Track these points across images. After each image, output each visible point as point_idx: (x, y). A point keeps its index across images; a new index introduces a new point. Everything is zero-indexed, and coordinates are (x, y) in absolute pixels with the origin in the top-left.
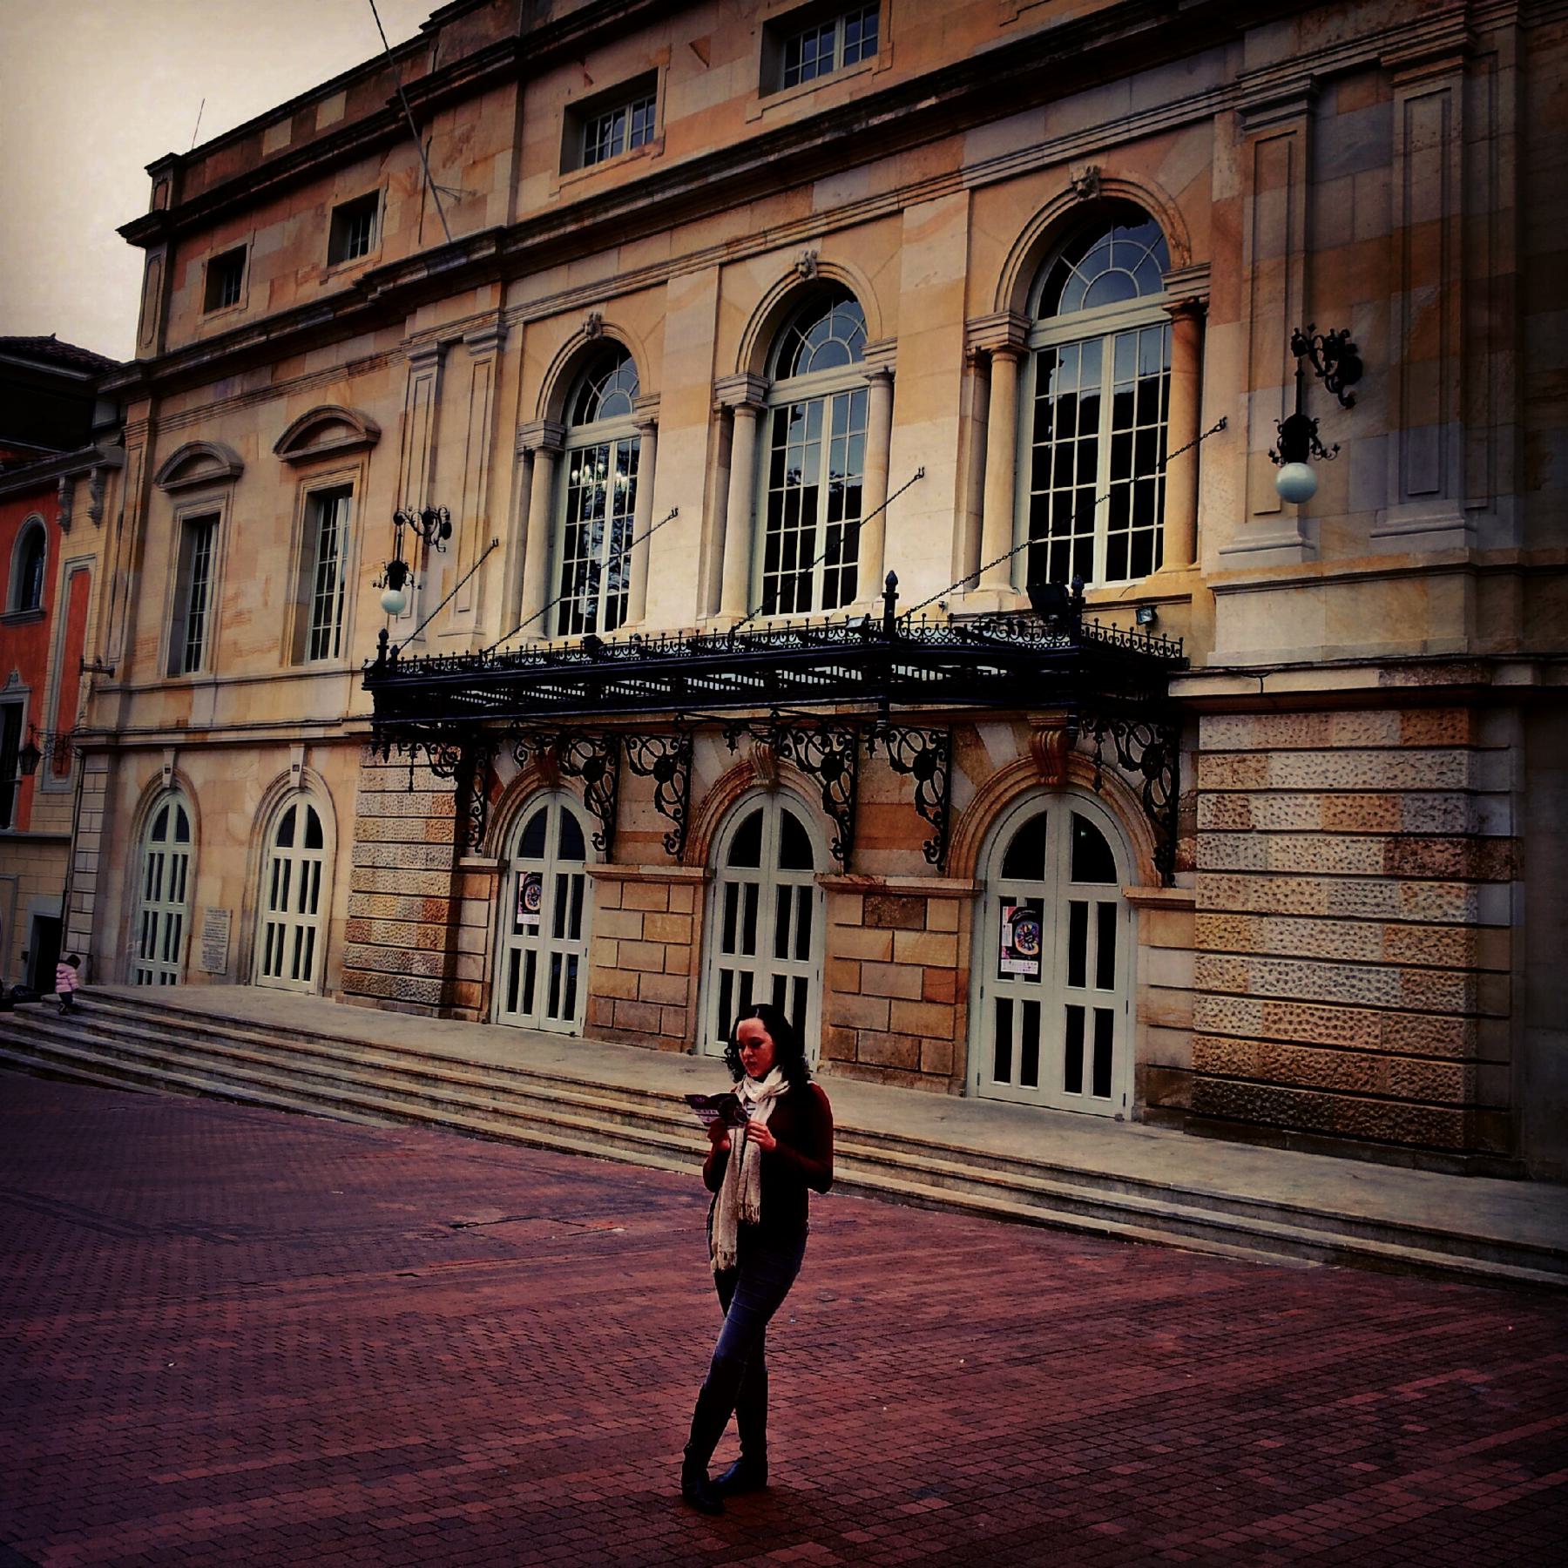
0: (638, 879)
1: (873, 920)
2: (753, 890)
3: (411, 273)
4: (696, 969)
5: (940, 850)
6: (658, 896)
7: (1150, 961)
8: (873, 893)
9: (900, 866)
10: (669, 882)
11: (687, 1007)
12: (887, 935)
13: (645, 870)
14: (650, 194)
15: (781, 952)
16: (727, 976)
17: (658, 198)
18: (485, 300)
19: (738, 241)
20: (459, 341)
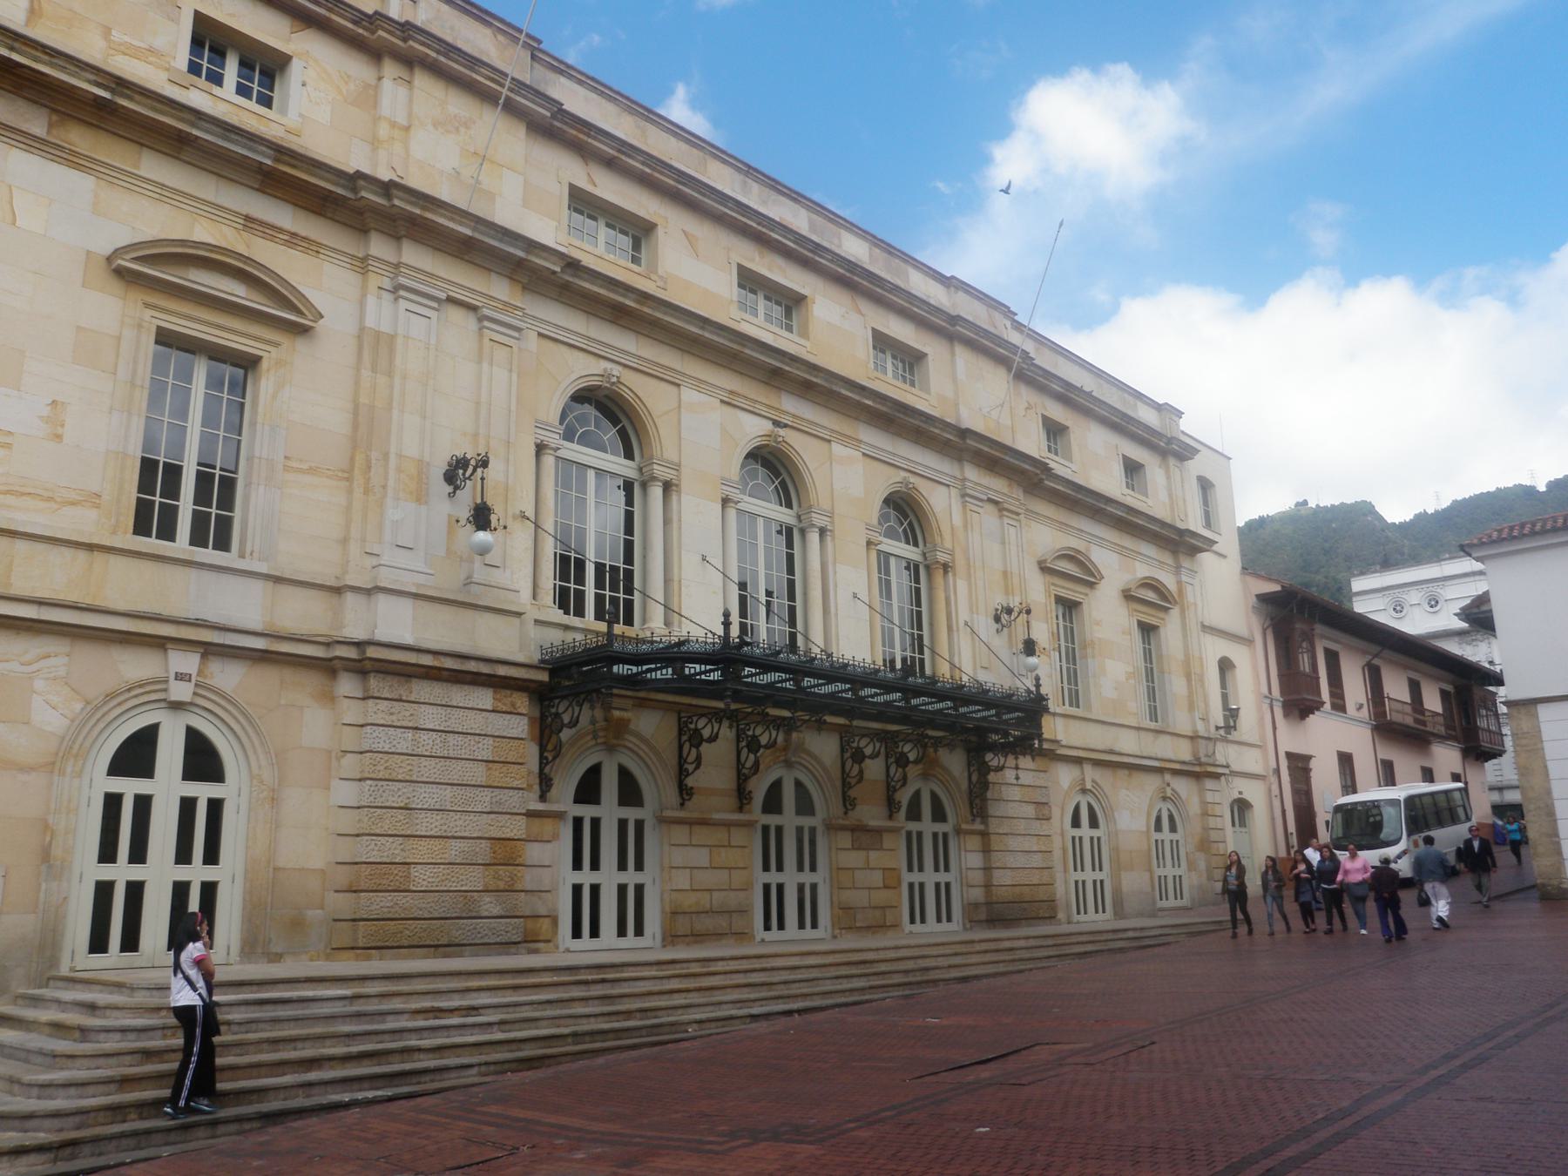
0: (704, 822)
1: (856, 847)
2: (779, 829)
3: (452, 219)
4: (747, 888)
5: (892, 806)
6: (720, 835)
7: (968, 858)
8: (858, 830)
9: (871, 814)
10: (728, 825)
11: (744, 911)
12: (863, 854)
13: (716, 816)
14: (702, 328)
15: (800, 868)
16: (767, 888)
17: (707, 335)
18: (501, 289)
19: (739, 395)
20: (473, 308)
